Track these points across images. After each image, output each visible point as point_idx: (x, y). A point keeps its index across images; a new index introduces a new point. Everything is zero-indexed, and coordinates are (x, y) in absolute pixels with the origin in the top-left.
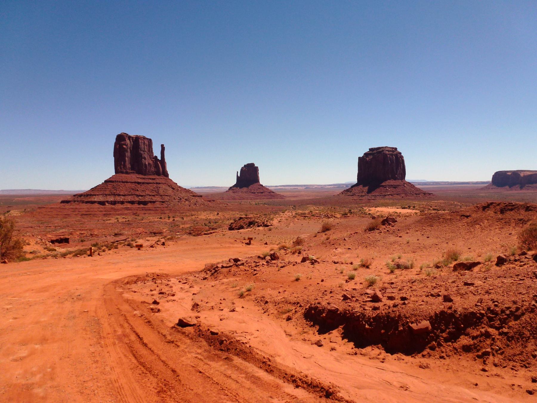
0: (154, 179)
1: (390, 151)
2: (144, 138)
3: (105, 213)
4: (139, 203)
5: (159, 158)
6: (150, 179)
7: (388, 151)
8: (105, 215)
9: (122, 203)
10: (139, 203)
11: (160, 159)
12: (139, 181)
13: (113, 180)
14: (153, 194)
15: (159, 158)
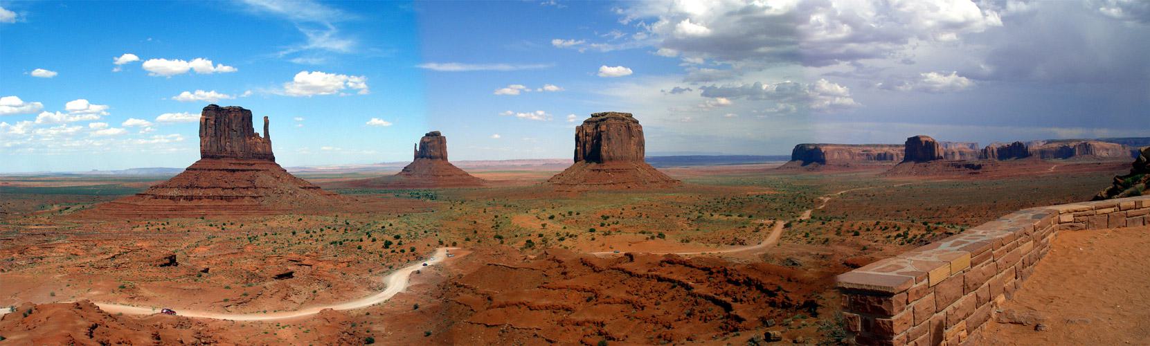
0: (252, 165)
1: (619, 119)
2: (241, 110)
3: (167, 212)
4: (221, 198)
5: (262, 135)
6: (248, 164)
7: (615, 119)
8: (166, 216)
9: (200, 198)
10: (221, 198)
11: (263, 136)
12: (233, 167)
13: (197, 167)
14: (243, 186)
15: (262, 135)
